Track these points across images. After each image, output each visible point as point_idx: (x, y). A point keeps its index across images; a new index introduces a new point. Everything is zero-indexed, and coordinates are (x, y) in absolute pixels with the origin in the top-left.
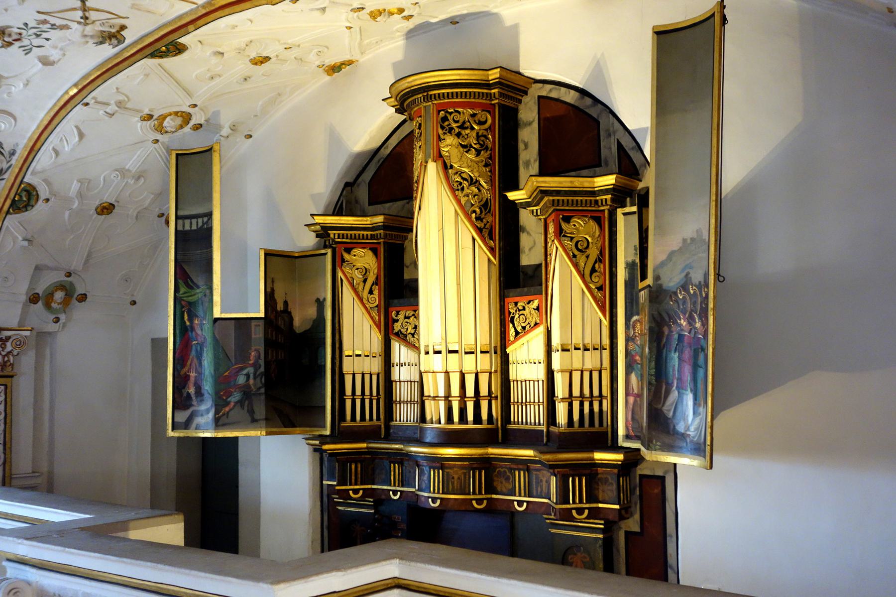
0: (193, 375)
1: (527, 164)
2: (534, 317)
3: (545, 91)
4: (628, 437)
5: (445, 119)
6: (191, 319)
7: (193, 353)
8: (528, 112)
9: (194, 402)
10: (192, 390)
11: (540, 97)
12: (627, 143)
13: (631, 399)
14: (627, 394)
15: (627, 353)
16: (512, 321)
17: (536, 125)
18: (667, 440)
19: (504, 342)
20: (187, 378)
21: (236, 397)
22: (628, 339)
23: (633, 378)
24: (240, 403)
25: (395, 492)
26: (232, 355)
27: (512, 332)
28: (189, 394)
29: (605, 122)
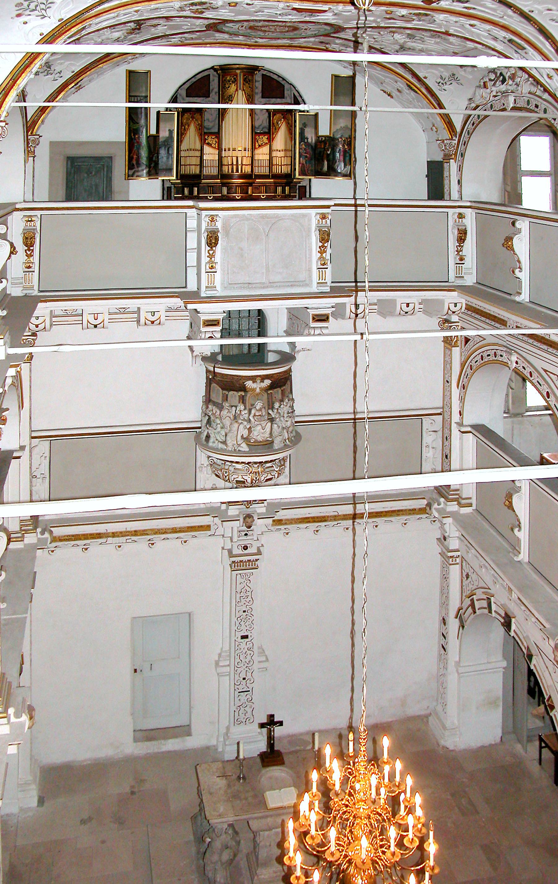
0: (135, 156)
1: (257, 93)
2: (266, 141)
3: (265, 73)
4: (299, 175)
5: (246, 78)
6: (134, 135)
7: (135, 148)
8: (258, 77)
9: (136, 167)
10: (134, 162)
11: (263, 75)
12: (296, 94)
13: (301, 165)
14: (299, 163)
15: (299, 152)
16: (257, 141)
17: (261, 82)
18: (335, 174)
19: (253, 148)
20: (133, 158)
21: (153, 165)
22: (300, 149)
23: (301, 159)
24: (154, 167)
25: (210, 197)
26: (152, 149)
27: (257, 144)
28: (133, 164)
29: (287, 86)
